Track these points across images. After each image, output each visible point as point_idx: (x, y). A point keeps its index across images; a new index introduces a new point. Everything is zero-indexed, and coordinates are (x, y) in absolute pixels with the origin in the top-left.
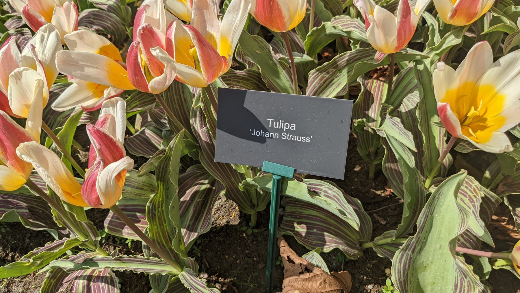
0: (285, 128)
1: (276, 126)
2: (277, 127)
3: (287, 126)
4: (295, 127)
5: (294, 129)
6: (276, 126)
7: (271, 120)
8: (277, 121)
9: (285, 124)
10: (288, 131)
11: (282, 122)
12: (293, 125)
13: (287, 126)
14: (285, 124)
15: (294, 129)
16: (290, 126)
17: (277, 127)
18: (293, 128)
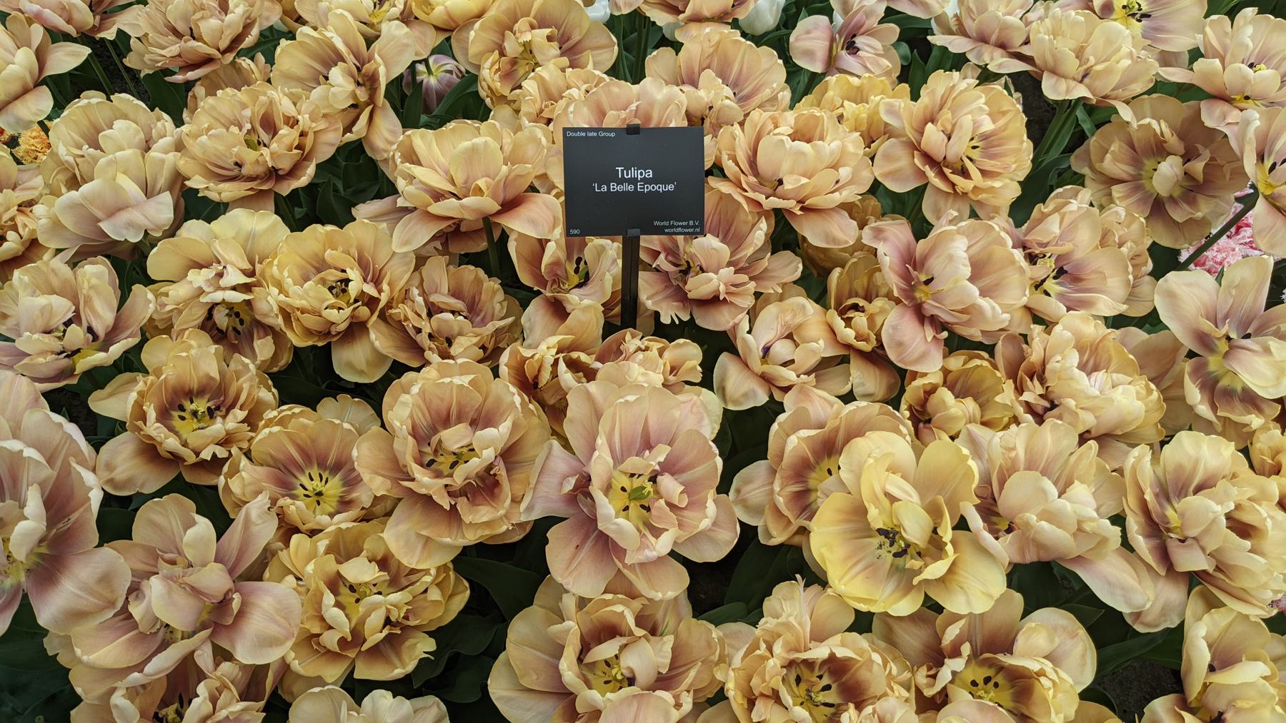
8: (628, 169)
10: (645, 181)
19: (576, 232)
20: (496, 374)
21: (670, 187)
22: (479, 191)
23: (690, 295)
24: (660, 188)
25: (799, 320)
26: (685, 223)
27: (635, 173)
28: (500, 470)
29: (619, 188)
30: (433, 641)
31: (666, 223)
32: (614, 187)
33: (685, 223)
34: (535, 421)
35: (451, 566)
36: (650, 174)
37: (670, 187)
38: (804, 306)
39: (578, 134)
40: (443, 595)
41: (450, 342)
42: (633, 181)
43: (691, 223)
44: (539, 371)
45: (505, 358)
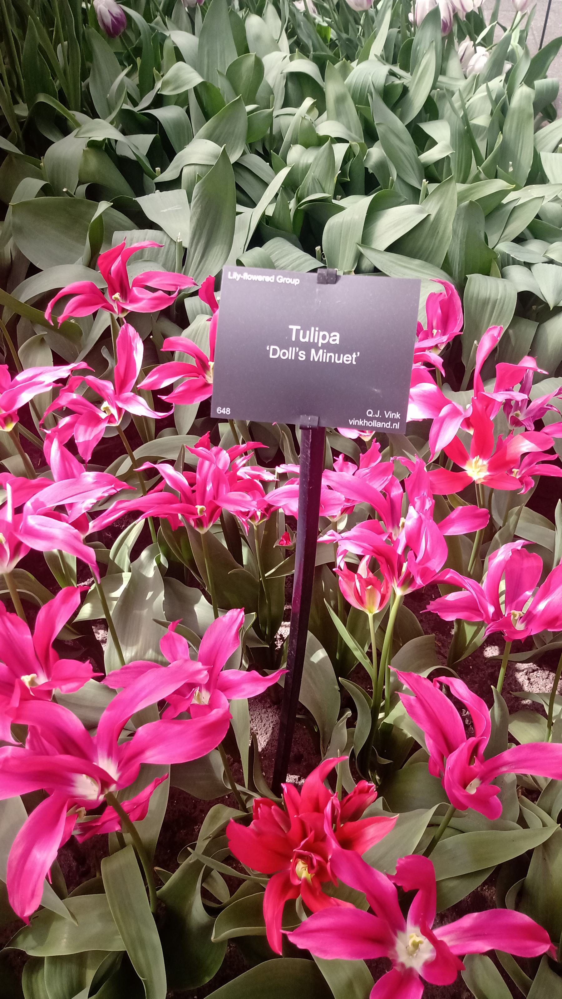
0: (321, 341)
1: (304, 337)
2: (307, 340)
3: (324, 337)
4: (338, 338)
5: (337, 342)
6: (304, 337)
7: (294, 328)
8: (306, 328)
10: (328, 347)
11: (315, 330)
12: (335, 336)
13: (324, 337)
15: (337, 342)
16: (330, 337)
18: (334, 340)
27: (314, 335)
29: (289, 354)
36: (335, 338)
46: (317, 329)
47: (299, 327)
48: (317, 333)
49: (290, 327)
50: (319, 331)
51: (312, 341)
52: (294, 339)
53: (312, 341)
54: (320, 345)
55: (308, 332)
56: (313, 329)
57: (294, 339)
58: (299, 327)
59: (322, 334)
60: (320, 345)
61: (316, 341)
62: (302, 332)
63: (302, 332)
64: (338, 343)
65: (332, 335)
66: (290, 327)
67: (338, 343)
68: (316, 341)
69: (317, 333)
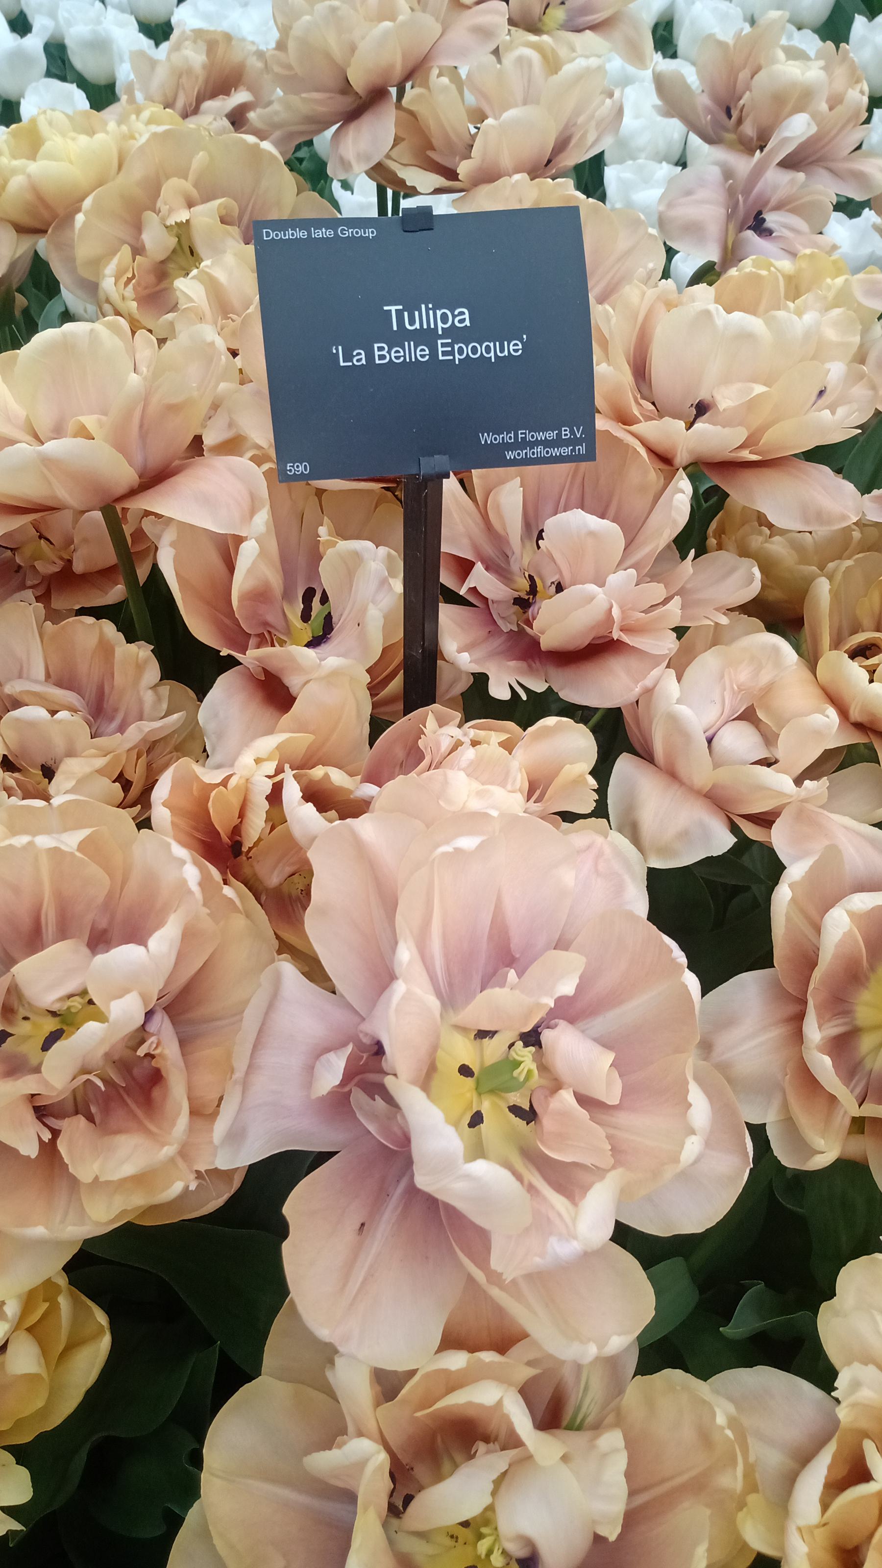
0: (440, 325)
1: (412, 322)
4: (467, 316)
6: (412, 322)
7: (393, 308)
8: (411, 307)
9: (439, 313)
10: (454, 333)
11: (427, 309)
12: (462, 313)
14: (439, 313)
16: (454, 316)
17: (417, 326)
18: (461, 321)
19: (301, 468)
20: (144, 823)
21: (514, 348)
22: (84, 433)
23: (546, 643)
24: (490, 350)
25: (765, 678)
26: (551, 435)
27: (427, 317)
28: (165, 1044)
30: (23, 1475)
31: (508, 437)
32: (384, 354)
33: (551, 435)
34: (239, 922)
35: (62, 1281)
36: (463, 317)
37: (514, 348)
38: (776, 650)
39: (289, 234)
40: (45, 1351)
41: (49, 773)
42: (427, 337)
43: (566, 433)
44: (242, 815)
45: (161, 792)
46: (430, 306)
47: (401, 307)
48: (431, 312)
49: (386, 308)
50: (434, 310)
51: (425, 327)
52: (395, 328)
53: (425, 327)
54: (440, 332)
55: (417, 313)
56: (423, 306)
57: (395, 328)
58: (401, 307)
59: (439, 313)
60: (440, 332)
61: (432, 326)
62: (406, 314)
63: (406, 314)
64: (469, 325)
65: (456, 313)
66: (386, 308)
67: (469, 325)
68: (432, 326)
69: (431, 312)
